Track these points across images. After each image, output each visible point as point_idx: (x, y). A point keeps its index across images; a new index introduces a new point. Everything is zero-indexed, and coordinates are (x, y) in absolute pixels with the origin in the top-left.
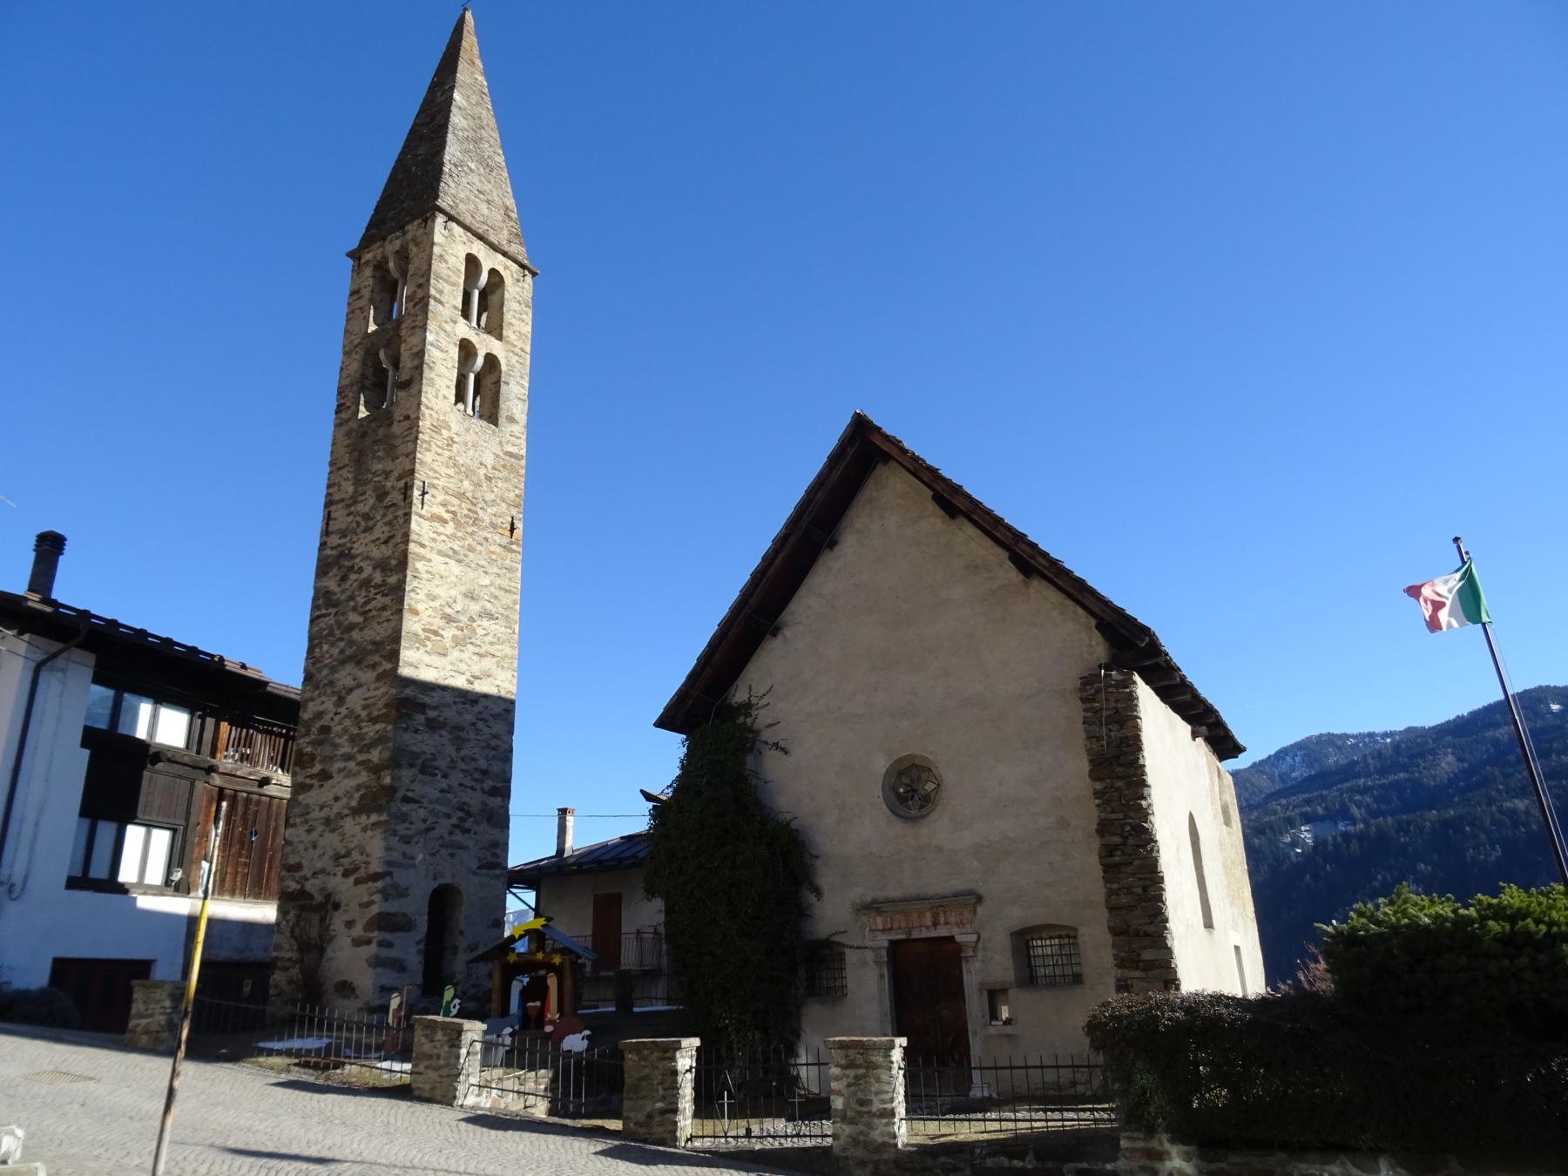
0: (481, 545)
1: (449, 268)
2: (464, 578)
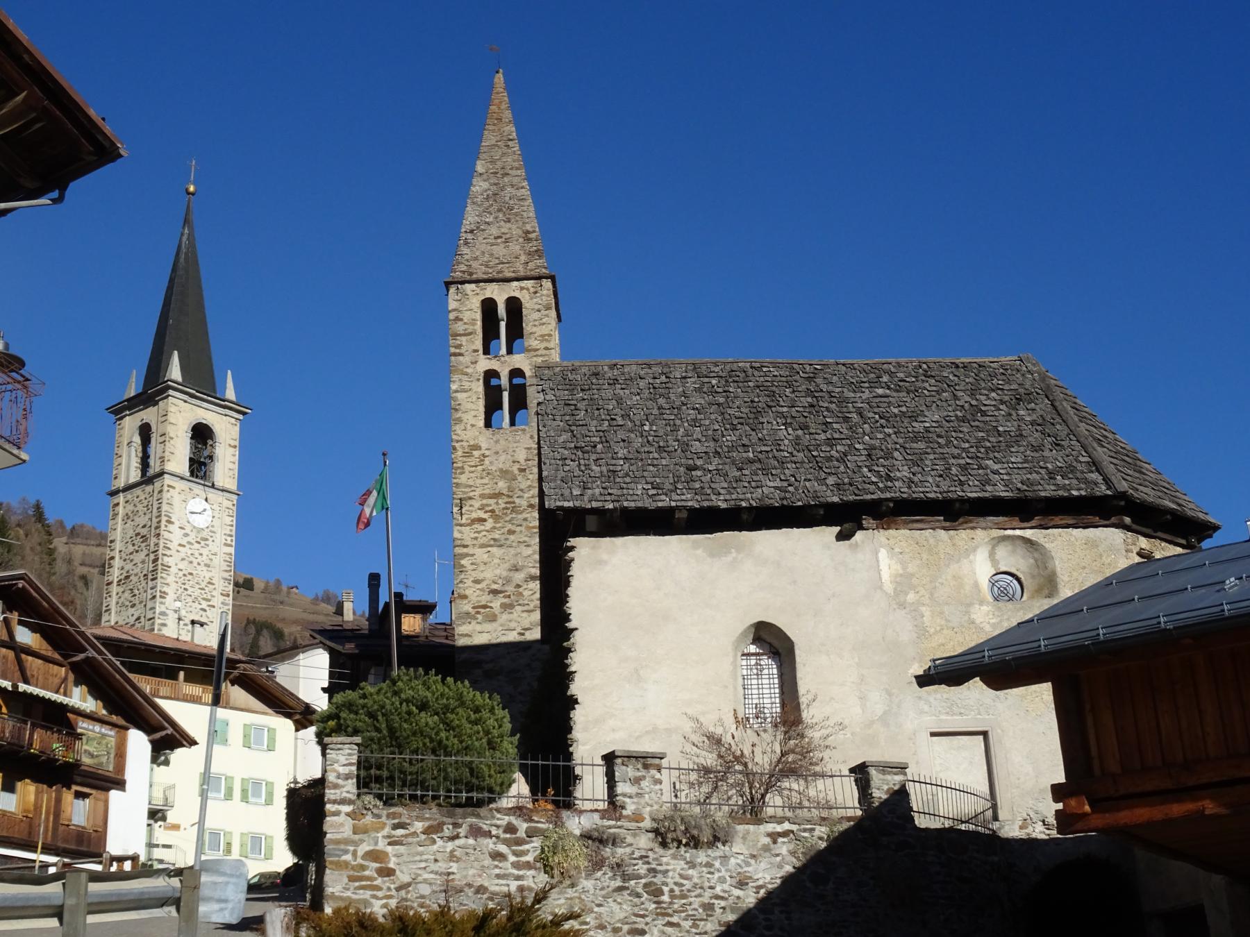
0: (521, 525)
1: (465, 323)
2: (506, 558)
